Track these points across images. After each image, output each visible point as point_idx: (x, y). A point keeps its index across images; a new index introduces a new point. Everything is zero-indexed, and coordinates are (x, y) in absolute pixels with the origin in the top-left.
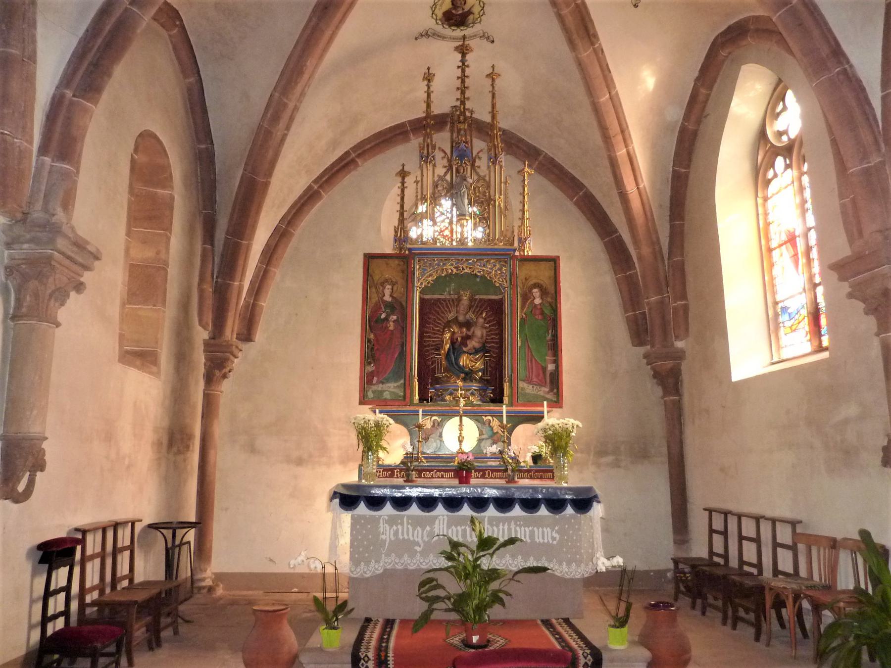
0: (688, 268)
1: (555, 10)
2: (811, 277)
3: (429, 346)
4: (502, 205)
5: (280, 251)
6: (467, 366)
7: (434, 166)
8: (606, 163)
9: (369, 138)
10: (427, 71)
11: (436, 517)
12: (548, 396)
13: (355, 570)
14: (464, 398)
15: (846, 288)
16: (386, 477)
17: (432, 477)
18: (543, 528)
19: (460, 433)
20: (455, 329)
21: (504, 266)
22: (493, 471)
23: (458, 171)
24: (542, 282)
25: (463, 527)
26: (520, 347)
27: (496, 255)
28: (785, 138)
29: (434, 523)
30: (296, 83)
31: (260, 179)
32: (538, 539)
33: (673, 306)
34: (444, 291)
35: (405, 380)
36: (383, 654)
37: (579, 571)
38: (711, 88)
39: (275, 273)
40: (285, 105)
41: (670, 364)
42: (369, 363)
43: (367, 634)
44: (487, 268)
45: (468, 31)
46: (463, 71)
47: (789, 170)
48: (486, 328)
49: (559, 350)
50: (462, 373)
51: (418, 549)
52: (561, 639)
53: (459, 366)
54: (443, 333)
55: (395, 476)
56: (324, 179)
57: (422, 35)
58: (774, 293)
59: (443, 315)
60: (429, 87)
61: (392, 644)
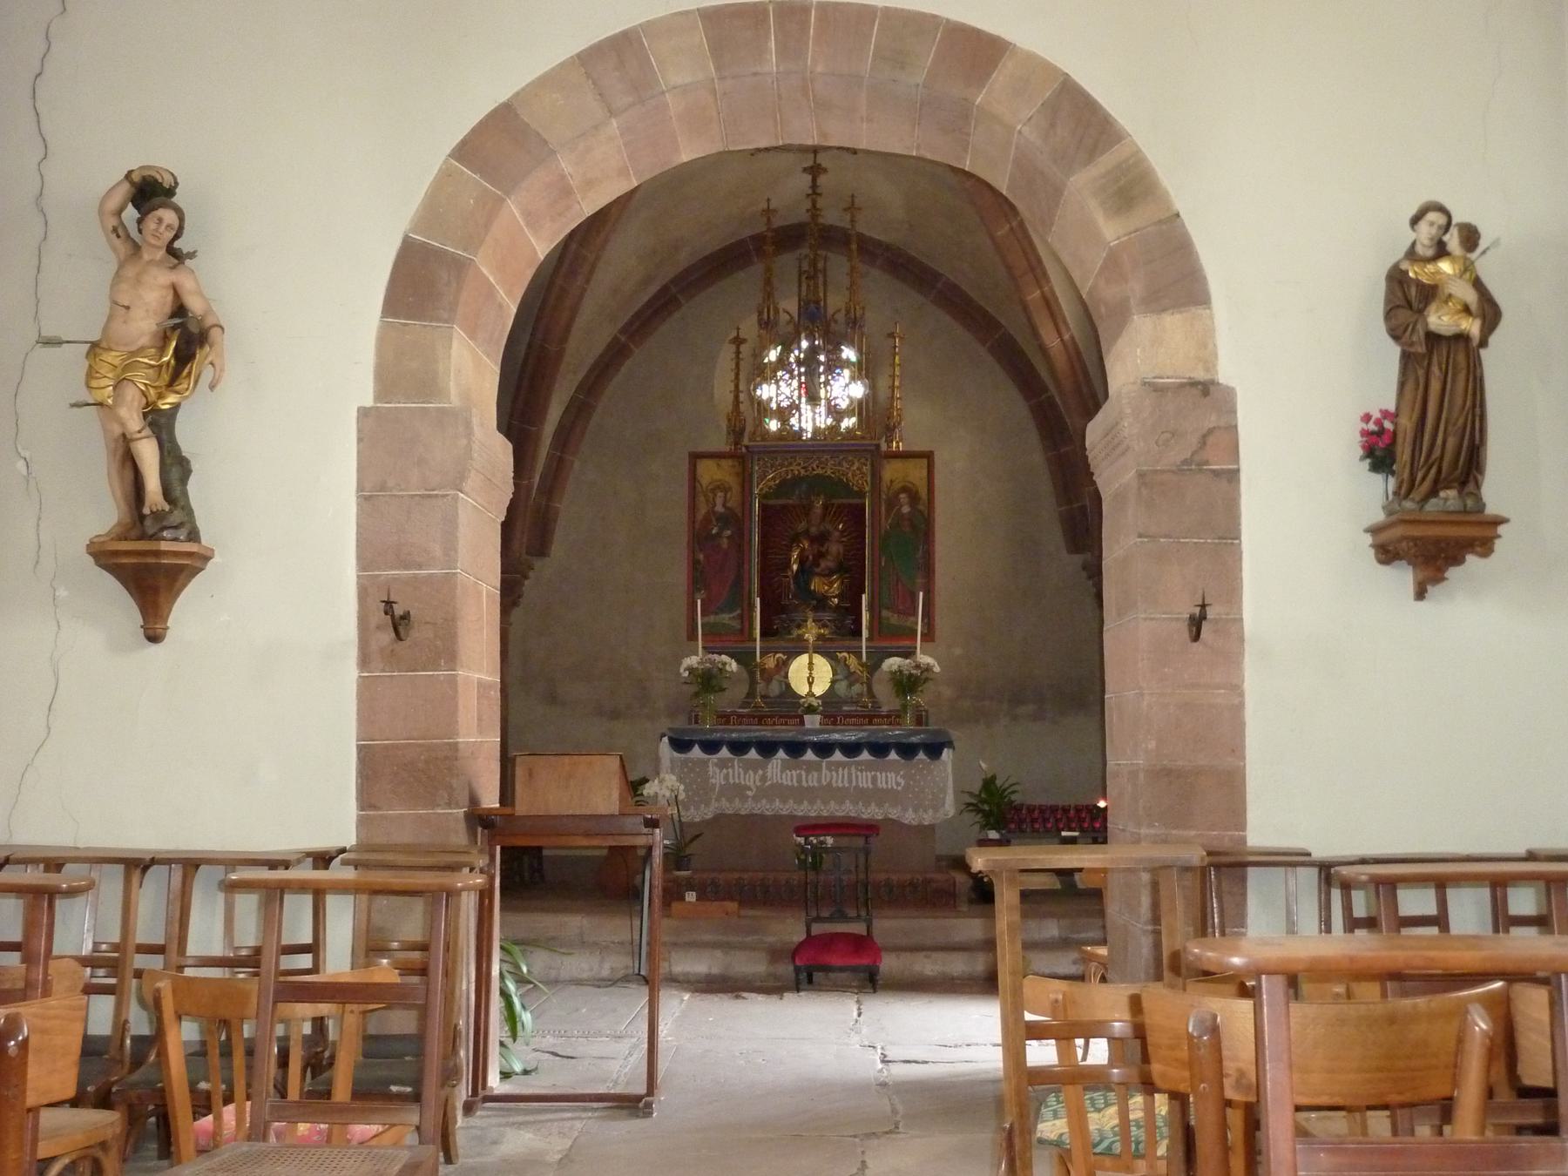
17: (774, 724)
18: (886, 772)
22: (846, 717)
24: (910, 485)
25: (798, 772)
32: (882, 784)
35: (742, 610)
50: (813, 599)
51: (749, 793)
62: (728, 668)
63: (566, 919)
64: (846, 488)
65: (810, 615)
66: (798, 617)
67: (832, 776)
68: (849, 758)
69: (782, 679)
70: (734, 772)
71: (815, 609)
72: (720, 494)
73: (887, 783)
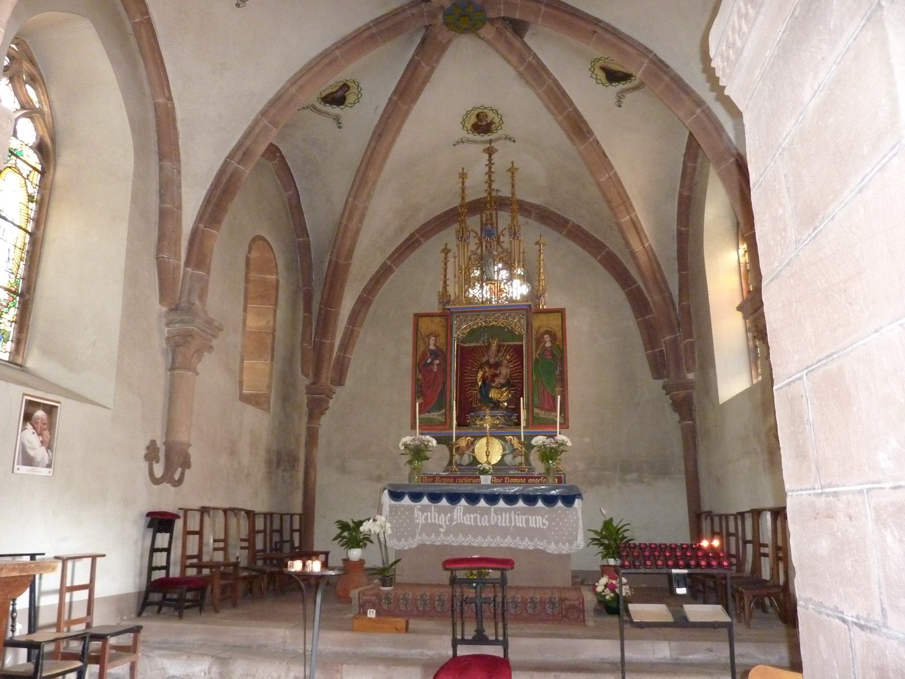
22: (511, 477)
24: (551, 329)
31: (342, 262)
32: (532, 525)
39: (359, 332)
45: (493, 136)
46: (490, 168)
51: (441, 530)
57: (458, 143)
62: (430, 444)
63: (274, 630)
64: (512, 333)
65: (488, 412)
66: (481, 413)
67: (498, 518)
69: (471, 454)
70: (431, 515)
71: (492, 409)
73: (536, 524)
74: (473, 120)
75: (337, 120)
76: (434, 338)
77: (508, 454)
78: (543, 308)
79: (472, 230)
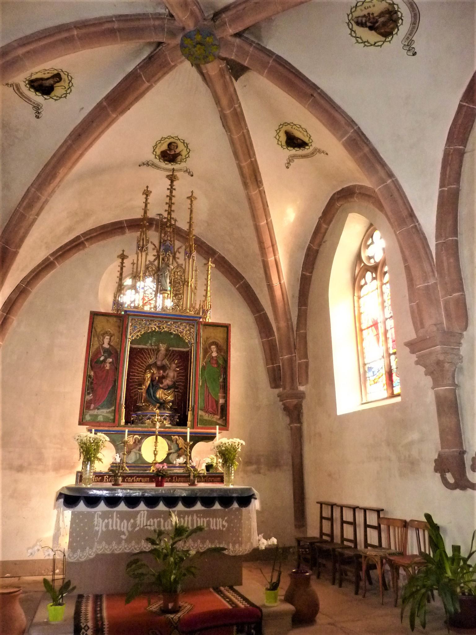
0: (309, 338)
1: (237, 162)
2: (387, 349)
3: (134, 382)
4: (193, 285)
5: (18, 304)
6: (162, 398)
7: (147, 254)
8: (261, 264)
9: (96, 228)
10: (146, 189)
11: (138, 512)
12: (219, 422)
13: (73, 556)
14: (160, 422)
15: (414, 357)
16: (98, 482)
17: (133, 482)
18: (216, 518)
19: (156, 448)
20: (154, 370)
21: (193, 328)
22: (178, 477)
23: (163, 259)
26: (201, 386)
27: (187, 320)
28: (372, 261)
29: (136, 517)
30: (50, 184)
33: (298, 363)
34: (147, 342)
35: (115, 408)
36: (100, 623)
37: (241, 550)
38: (329, 224)
39: (13, 320)
40: (38, 198)
41: (295, 401)
42: (89, 394)
43: (83, 608)
44: (180, 328)
45: (176, 166)
47: (375, 281)
48: (176, 371)
49: (228, 389)
50: (158, 403)
52: (231, 602)
53: (156, 398)
54: (145, 372)
55: (105, 481)
56: (59, 254)
57: (144, 164)
58: (363, 358)
59: (145, 360)
60: (147, 199)
61: (105, 614)
68: (187, 507)
69: (137, 452)
70: (113, 521)
72: (107, 337)
74: (164, 147)
75: (37, 109)
76: (107, 337)
77: (174, 453)
78: (208, 322)
79: (151, 242)
